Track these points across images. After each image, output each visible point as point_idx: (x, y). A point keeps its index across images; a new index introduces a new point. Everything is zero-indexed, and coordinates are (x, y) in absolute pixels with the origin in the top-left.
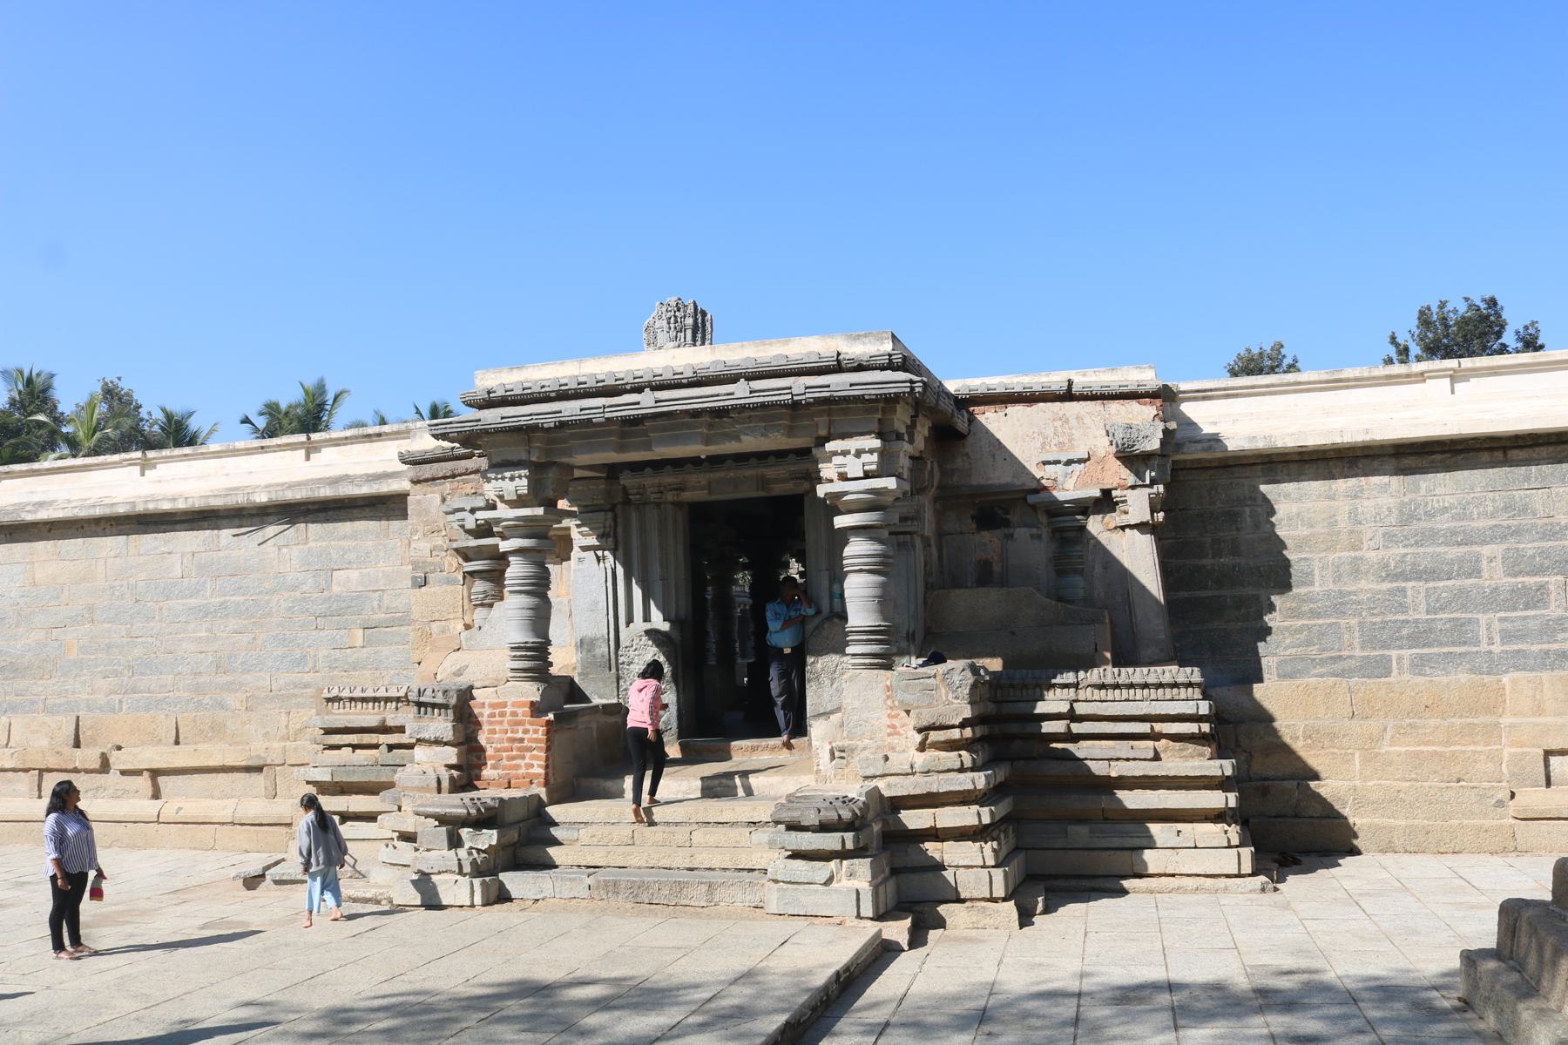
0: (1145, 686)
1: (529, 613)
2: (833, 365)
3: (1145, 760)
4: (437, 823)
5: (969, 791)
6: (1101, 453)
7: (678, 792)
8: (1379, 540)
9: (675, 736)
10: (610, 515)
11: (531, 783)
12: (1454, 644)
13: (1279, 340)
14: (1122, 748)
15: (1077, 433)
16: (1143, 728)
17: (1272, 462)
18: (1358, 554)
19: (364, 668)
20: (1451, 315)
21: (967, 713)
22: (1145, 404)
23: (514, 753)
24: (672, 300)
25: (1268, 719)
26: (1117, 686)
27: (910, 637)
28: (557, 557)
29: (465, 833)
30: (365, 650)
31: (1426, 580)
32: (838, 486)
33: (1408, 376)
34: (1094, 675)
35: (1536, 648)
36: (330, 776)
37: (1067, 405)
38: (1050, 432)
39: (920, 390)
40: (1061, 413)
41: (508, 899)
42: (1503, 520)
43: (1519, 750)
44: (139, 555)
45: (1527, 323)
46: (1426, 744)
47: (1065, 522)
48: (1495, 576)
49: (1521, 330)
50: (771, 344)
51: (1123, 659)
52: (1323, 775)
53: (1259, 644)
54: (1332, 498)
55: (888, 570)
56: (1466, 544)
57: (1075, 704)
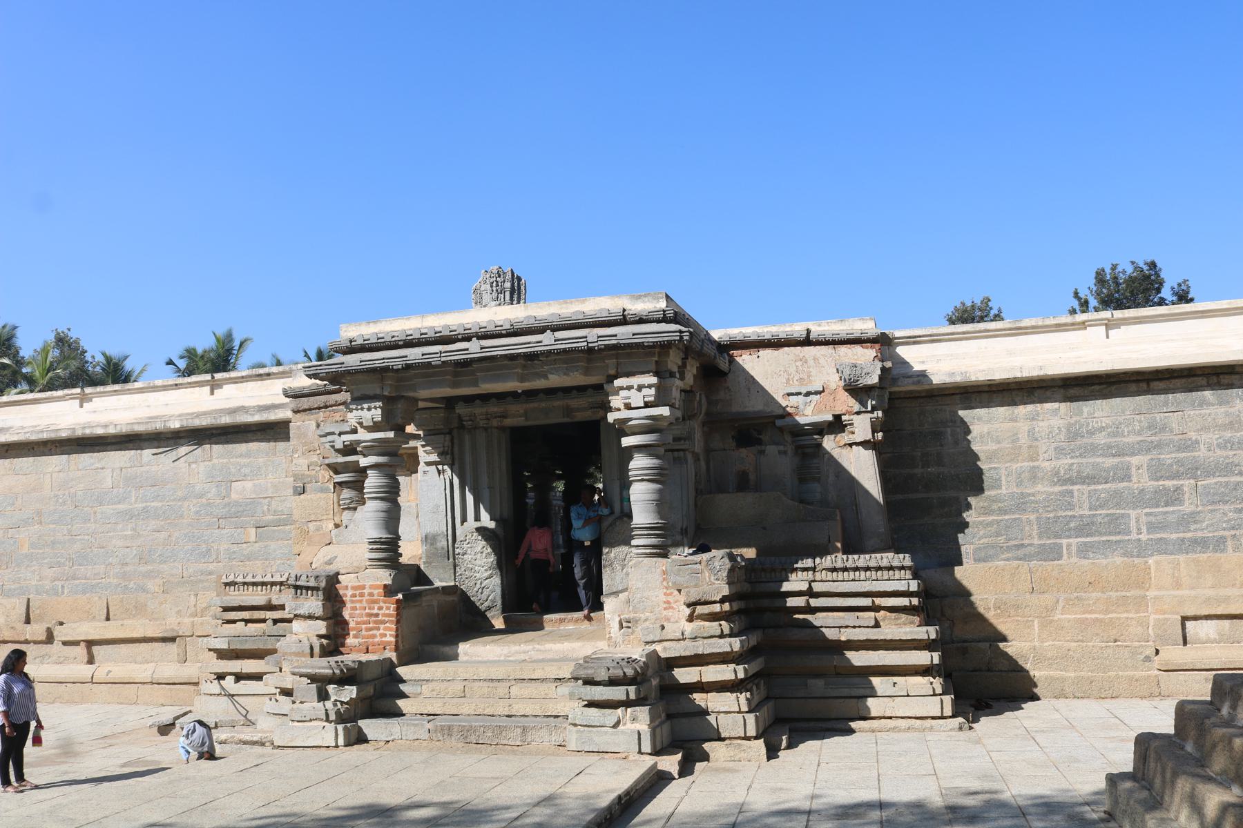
0: (868, 569)
1: (382, 515)
2: (620, 319)
3: (868, 627)
4: (309, 681)
5: (727, 653)
6: (833, 386)
7: (501, 655)
8: (1052, 453)
9: (500, 611)
10: (448, 437)
11: (385, 649)
12: (1111, 533)
13: (986, 296)
14: (849, 618)
15: (814, 372)
16: (866, 602)
18: (1036, 464)
19: (256, 559)
20: (1121, 275)
21: (726, 591)
22: (867, 348)
23: (371, 625)
24: (494, 269)
25: (967, 594)
26: (845, 569)
27: (684, 532)
28: (408, 471)
30: (257, 544)
31: (1089, 484)
33: (1073, 324)
34: (828, 561)
35: (1174, 536)
36: (227, 645)
37: (806, 348)
38: (792, 370)
39: (687, 338)
40: (801, 355)
41: (366, 741)
42: (1147, 437)
43: (1161, 617)
44: (78, 470)
45: (1180, 281)
46: (1090, 612)
47: (805, 440)
48: (1142, 480)
49: (1176, 287)
50: (571, 303)
52: (1009, 638)
53: (959, 535)
54: (1015, 420)
56: (1119, 456)
57: (812, 584)
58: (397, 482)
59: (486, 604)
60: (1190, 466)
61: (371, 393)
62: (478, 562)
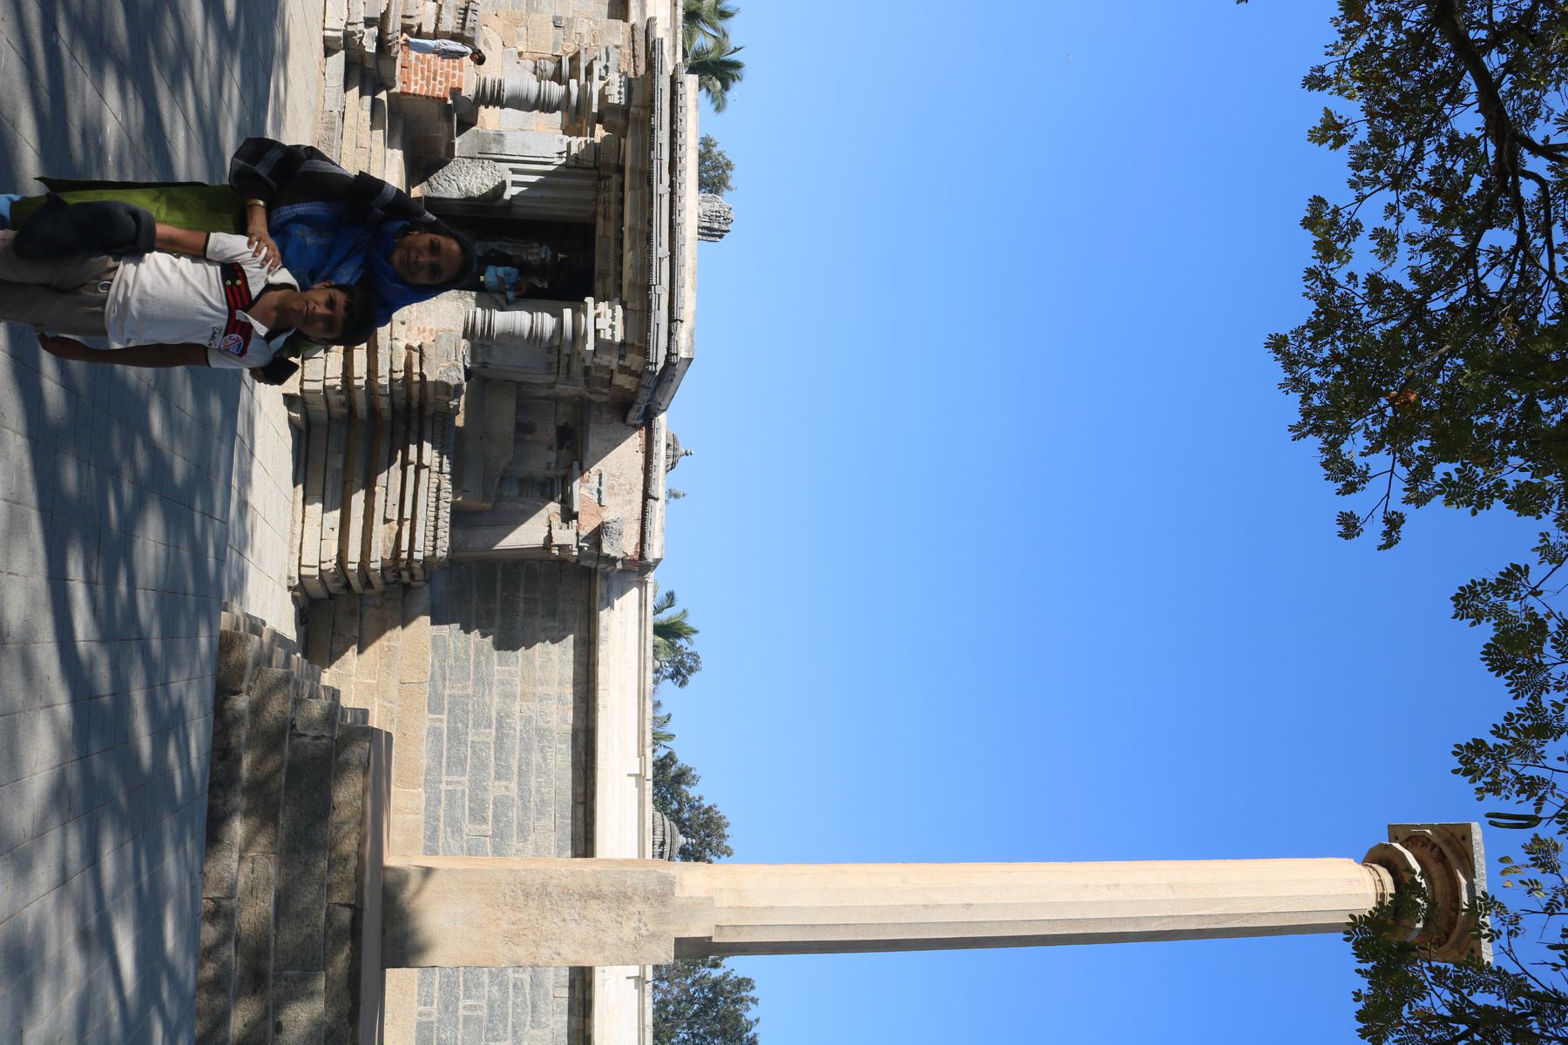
0: (437, 518)
1: (525, 94)
3: (385, 512)
4: (382, 12)
5: (377, 374)
8: (528, 713)
9: (426, 194)
10: (592, 165)
12: (449, 758)
16: (408, 513)
17: (589, 643)
18: (518, 698)
21: (429, 378)
22: (636, 548)
24: (731, 216)
25: (405, 624)
26: (438, 499)
27: (484, 365)
29: (375, 30)
31: (496, 743)
32: (591, 312)
33: (643, 746)
34: (447, 485)
35: (442, 813)
37: (641, 495)
39: (650, 369)
40: (635, 490)
41: (326, 55)
47: (558, 486)
48: (495, 789)
50: (693, 278)
51: (458, 515)
52: (361, 656)
53: (459, 625)
54: (560, 683)
55: (532, 341)
57: (427, 469)
58: (553, 111)
59: (434, 183)
60: (504, 831)
61: (634, 95)
62: (474, 180)
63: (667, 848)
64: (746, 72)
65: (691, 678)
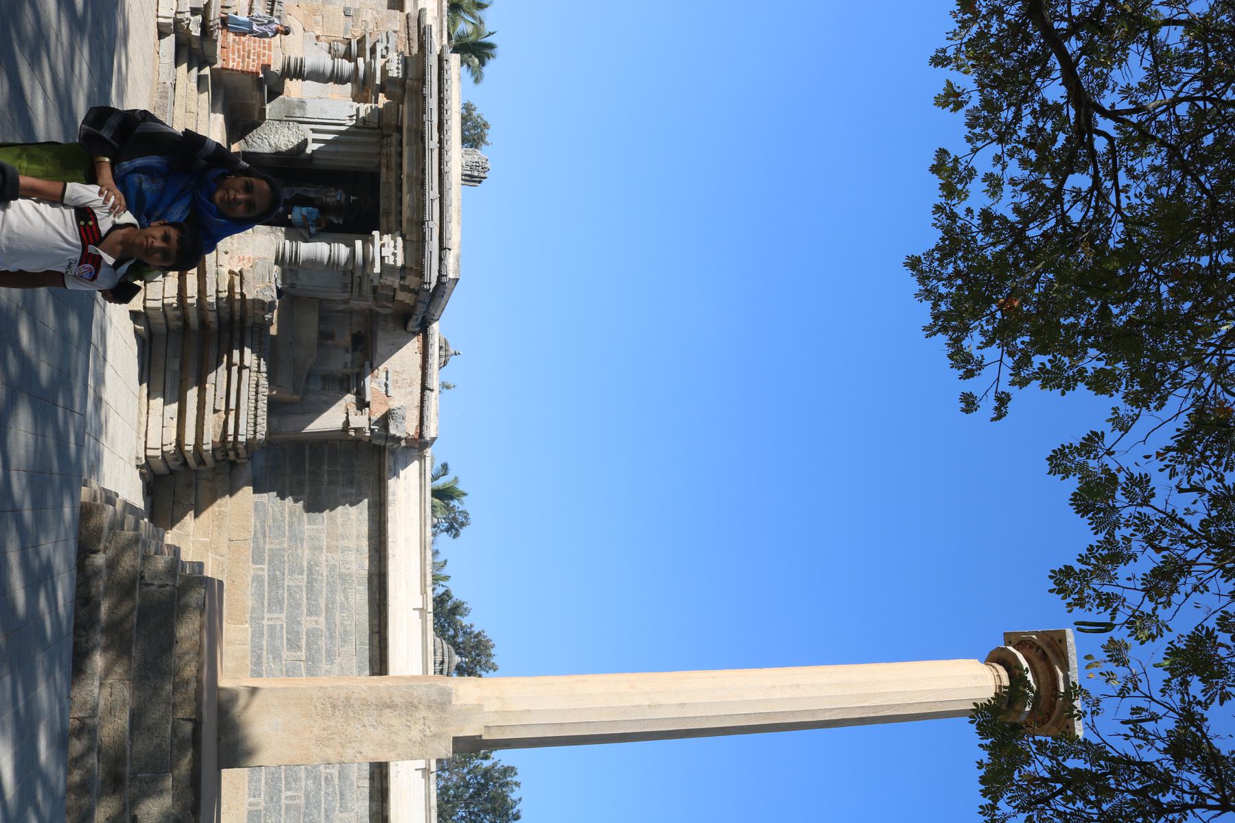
0: (256, 408)
8: (332, 562)
10: (376, 125)
11: (224, 60)
12: (269, 599)
14: (222, 392)
15: (402, 391)
16: (233, 405)
17: (380, 506)
18: (324, 550)
21: (248, 297)
22: (416, 429)
25: (232, 493)
26: (257, 393)
27: (293, 286)
29: (199, 18)
31: (307, 586)
32: (377, 242)
33: (425, 585)
34: (264, 382)
35: (265, 643)
37: (419, 387)
38: (404, 376)
41: (160, 38)
42: (339, 630)
47: (353, 381)
48: (307, 623)
50: (459, 215)
51: (273, 405)
52: (197, 520)
54: (358, 538)
55: (330, 267)
57: (248, 370)
59: (250, 140)
62: (282, 138)
63: (446, 666)
64: (499, 51)
65: (463, 531)
